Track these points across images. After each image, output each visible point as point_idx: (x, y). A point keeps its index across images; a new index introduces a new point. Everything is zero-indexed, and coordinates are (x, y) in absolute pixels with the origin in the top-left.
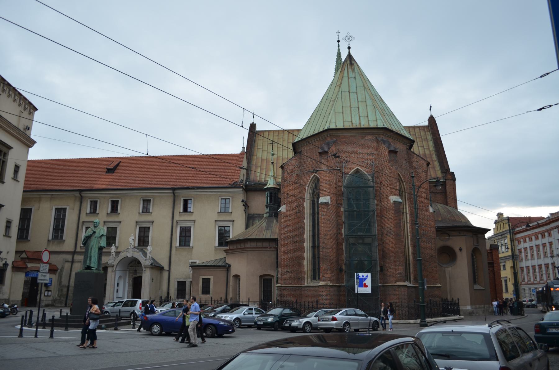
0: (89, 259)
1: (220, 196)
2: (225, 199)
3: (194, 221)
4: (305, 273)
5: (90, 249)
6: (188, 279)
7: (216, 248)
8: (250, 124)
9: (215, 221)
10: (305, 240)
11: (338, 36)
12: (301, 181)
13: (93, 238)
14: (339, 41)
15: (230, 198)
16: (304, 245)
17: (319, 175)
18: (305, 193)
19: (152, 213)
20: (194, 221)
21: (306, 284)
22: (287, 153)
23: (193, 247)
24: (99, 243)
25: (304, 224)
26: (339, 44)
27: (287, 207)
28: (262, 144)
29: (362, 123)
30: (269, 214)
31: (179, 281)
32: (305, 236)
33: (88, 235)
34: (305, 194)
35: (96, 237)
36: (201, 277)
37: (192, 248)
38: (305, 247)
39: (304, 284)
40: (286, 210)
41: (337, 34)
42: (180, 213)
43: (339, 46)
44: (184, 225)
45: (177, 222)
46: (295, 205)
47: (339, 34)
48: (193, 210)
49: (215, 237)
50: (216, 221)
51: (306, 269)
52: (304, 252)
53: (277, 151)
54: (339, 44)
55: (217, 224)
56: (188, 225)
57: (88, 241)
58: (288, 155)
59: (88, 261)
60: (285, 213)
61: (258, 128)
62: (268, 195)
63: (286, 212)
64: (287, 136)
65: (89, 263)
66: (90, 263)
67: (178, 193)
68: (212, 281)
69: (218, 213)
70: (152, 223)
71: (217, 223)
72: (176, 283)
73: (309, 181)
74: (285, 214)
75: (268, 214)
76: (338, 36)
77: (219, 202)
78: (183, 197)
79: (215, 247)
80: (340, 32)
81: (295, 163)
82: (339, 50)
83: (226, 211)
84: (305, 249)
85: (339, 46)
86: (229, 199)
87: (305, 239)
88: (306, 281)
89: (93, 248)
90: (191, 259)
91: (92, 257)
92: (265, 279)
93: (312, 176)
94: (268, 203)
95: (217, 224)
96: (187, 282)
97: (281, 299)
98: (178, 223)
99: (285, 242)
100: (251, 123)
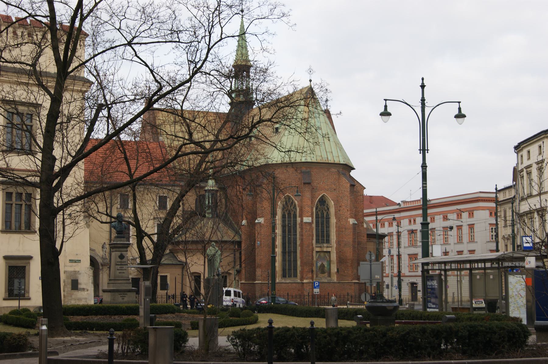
29: (329, 158)
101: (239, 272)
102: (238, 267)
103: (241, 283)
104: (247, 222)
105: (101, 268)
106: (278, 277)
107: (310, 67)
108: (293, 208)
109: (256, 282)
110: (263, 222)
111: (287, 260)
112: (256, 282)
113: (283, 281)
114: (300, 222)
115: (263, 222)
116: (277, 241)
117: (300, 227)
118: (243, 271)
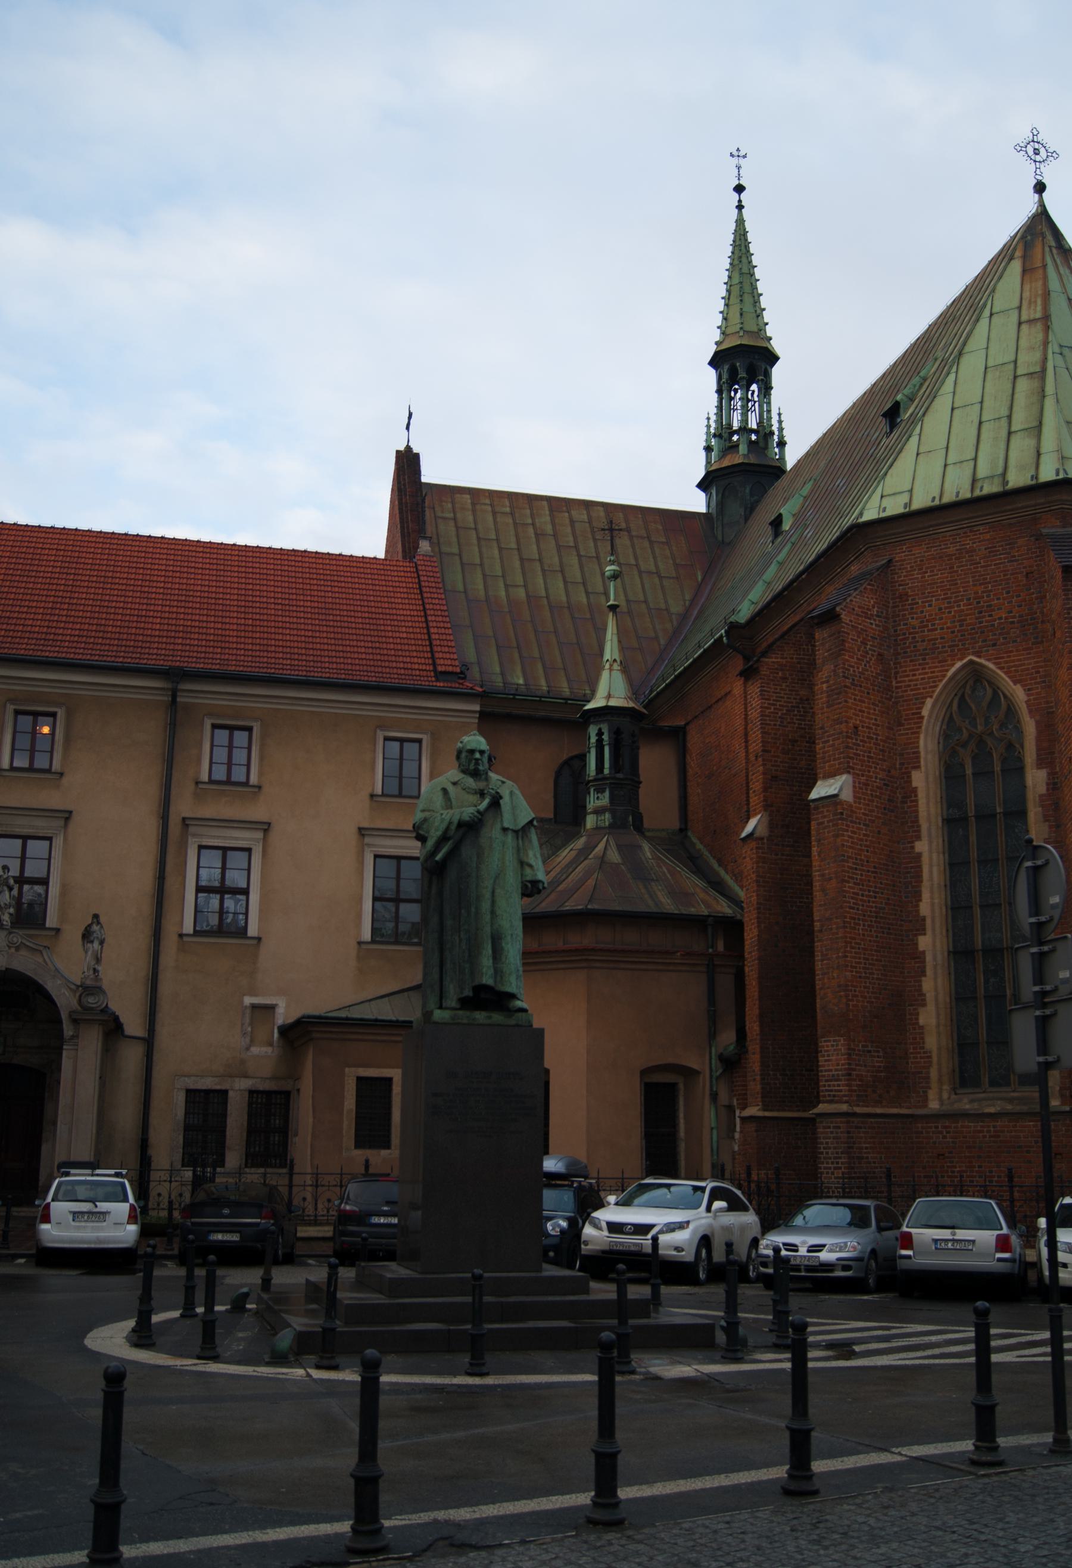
0: (488, 950)
1: (382, 727)
2: (402, 741)
3: (266, 828)
4: (931, 1062)
5: (488, 895)
6: (237, 1080)
7: (364, 946)
8: (398, 452)
9: (360, 829)
10: (924, 925)
11: (739, 168)
12: (894, 683)
13: (492, 833)
14: (739, 189)
15: (425, 738)
16: (917, 944)
17: (995, 664)
18: (918, 733)
19: (61, 774)
20: (266, 828)
21: (934, 1105)
22: (561, 585)
23: (259, 939)
24: (522, 864)
25: (920, 855)
26: (740, 201)
27: (857, 785)
28: (455, 539)
30: (614, 817)
31: (192, 1087)
32: (924, 909)
33: (466, 817)
34: (918, 738)
35: (505, 830)
36: (353, 1069)
37: (255, 942)
38: (924, 952)
39: (926, 1106)
40: (855, 797)
41: (735, 161)
42: (197, 783)
43: (740, 207)
44: (218, 837)
45: (185, 822)
46: (881, 779)
47: (742, 161)
48: (261, 774)
49: (360, 900)
50: (362, 832)
51: (931, 1042)
52: (923, 973)
53: (524, 574)
54: (740, 201)
55: (369, 845)
56: (236, 839)
57: (467, 851)
58: (567, 595)
59: (486, 961)
60: (851, 806)
61: (430, 474)
62: (605, 737)
63: (855, 802)
64: (548, 518)
65: (491, 971)
66: (498, 973)
67: (193, 694)
68: (397, 1089)
69: (372, 796)
70: (62, 823)
71: (367, 840)
72: (180, 1098)
73: (941, 685)
74: (852, 811)
75: (607, 815)
76: (739, 168)
77: (374, 751)
78: (210, 715)
79: (360, 943)
80: (745, 157)
81: (874, 607)
82: (740, 222)
83: (404, 793)
84: (924, 962)
85: (740, 207)
86: (419, 741)
87: (924, 919)
88: (932, 1094)
89: (498, 891)
90: (253, 993)
91: (509, 937)
92: (657, 1084)
93: (959, 664)
94: (606, 771)
95: (369, 845)
96: (231, 1094)
97: (853, 1168)
98: (192, 829)
99: (854, 928)
100: (402, 448)
101: (731, 1064)
102: (727, 1038)
103: (743, 1119)
104: (772, 826)
105: (68, 1030)
106: (934, 1085)
107: (1035, 132)
108: (1003, 725)
109: (822, 1108)
110: (847, 796)
111: (981, 992)
112: (822, 1108)
113: (965, 1104)
114: (1042, 789)
115: (847, 796)
116: (926, 895)
117: (1046, 818)
118: (754, 1060)
